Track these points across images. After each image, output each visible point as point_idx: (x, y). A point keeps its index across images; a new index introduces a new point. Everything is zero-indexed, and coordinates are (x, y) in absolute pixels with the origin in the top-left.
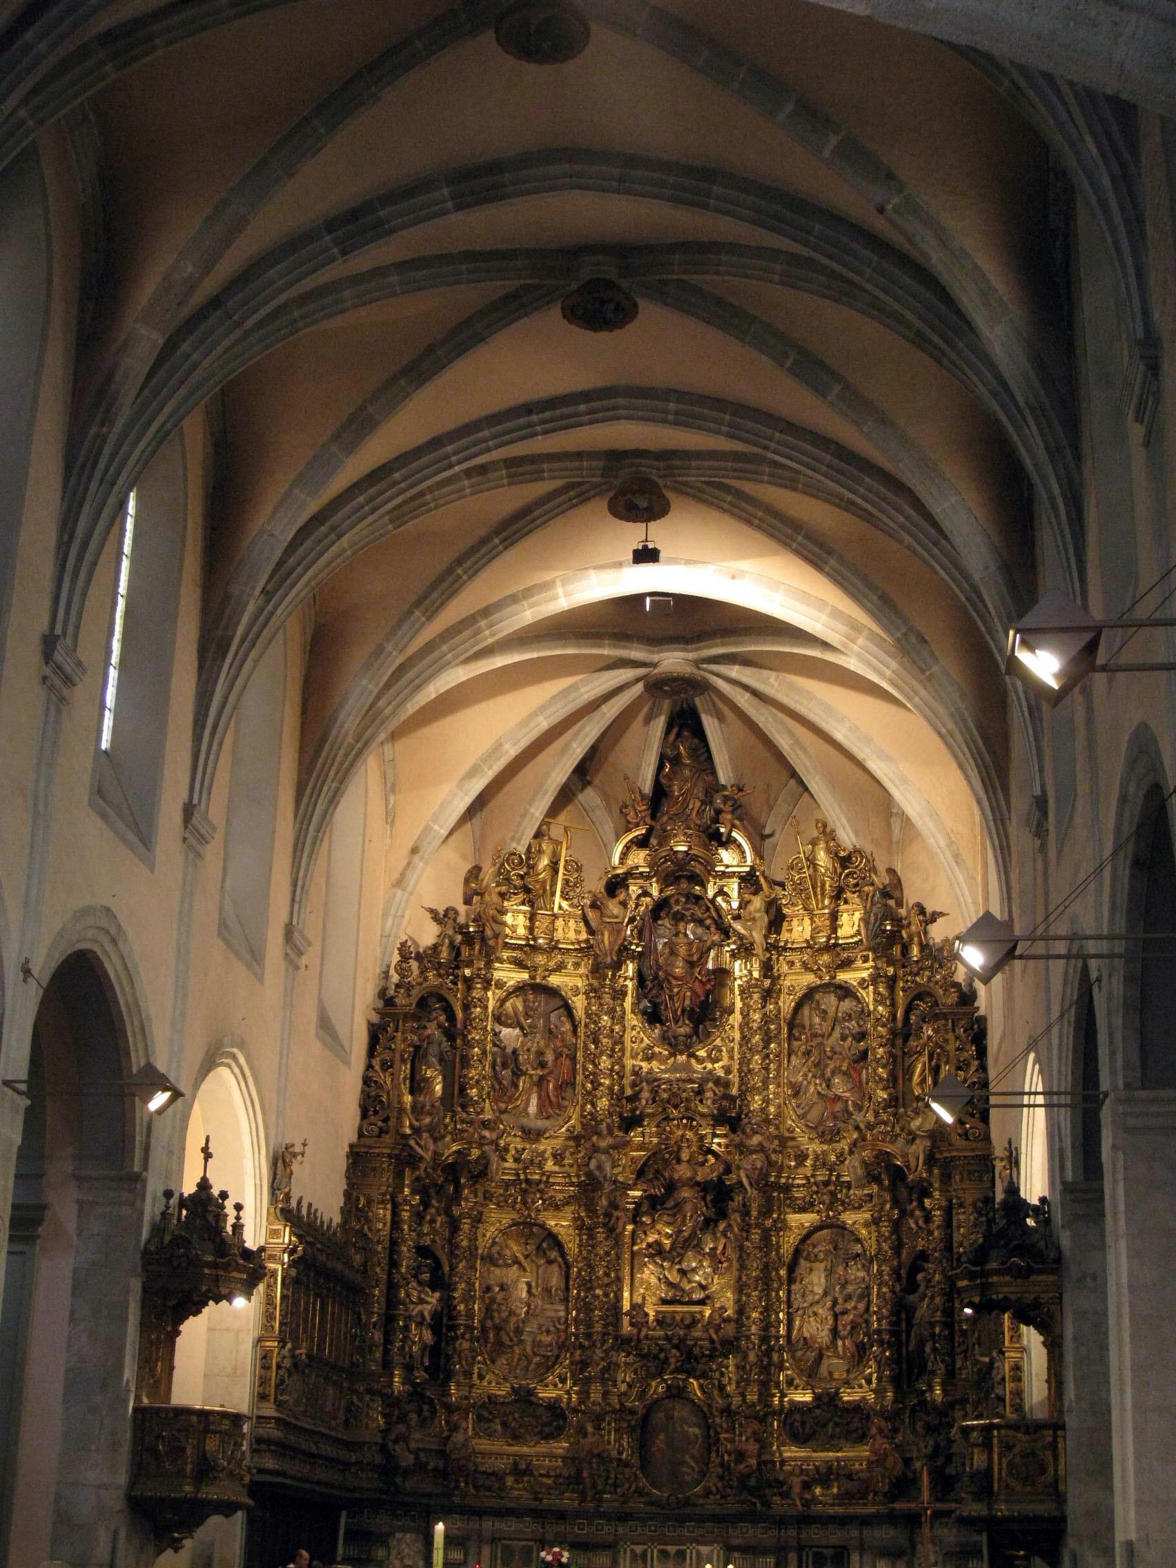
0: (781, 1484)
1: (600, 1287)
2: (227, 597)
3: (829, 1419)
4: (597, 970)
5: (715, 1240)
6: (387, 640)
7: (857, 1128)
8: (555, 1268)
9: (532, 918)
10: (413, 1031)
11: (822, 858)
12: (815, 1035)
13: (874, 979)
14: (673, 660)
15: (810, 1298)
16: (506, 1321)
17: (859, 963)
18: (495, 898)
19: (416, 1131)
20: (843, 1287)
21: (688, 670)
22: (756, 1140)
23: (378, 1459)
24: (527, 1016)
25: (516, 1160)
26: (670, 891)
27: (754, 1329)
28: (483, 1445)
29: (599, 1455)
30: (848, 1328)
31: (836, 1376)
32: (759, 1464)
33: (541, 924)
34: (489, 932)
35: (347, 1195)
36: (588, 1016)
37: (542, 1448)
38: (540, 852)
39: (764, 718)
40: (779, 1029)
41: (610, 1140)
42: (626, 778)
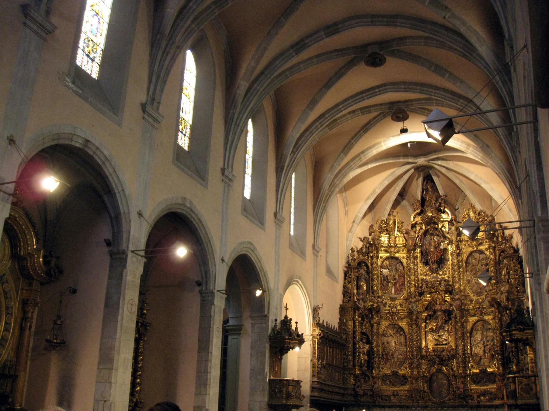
0: (471, 396)
2: (282, 154)
3: (484, 377)
4: (409, 251)
5: (448, 326)
6: (335, 162)
7: (486, 291)
8: (402, 336)
9: (389, 238)
10: (356, 272)
11: (472, 214)
12: (473, 265)
13: (489, 247)
14: (421, 161)
15: (477, 342)
16: (389, 352)
17: (485, 243)
18: (378, 233)
19: (358, 300)
20: (486, 338)
21: (425, 163)
22: (457, 297)
23: (353, 393)
24: (390, 266)
25: (389, 307)
26: (429, 227)
27: (460, 351)
28: (384, 387)
29: (417, 389)
31: (486, 364)
32: (464, 390)
33: (392, 240)
34: (376, 243)
35: (340, 319)
36: (407, 264)
37: (401, 388)
38: (390, 219)
39: (450, 175)
40: (463, 264)
41: (415, 299)
42: (413, 196)
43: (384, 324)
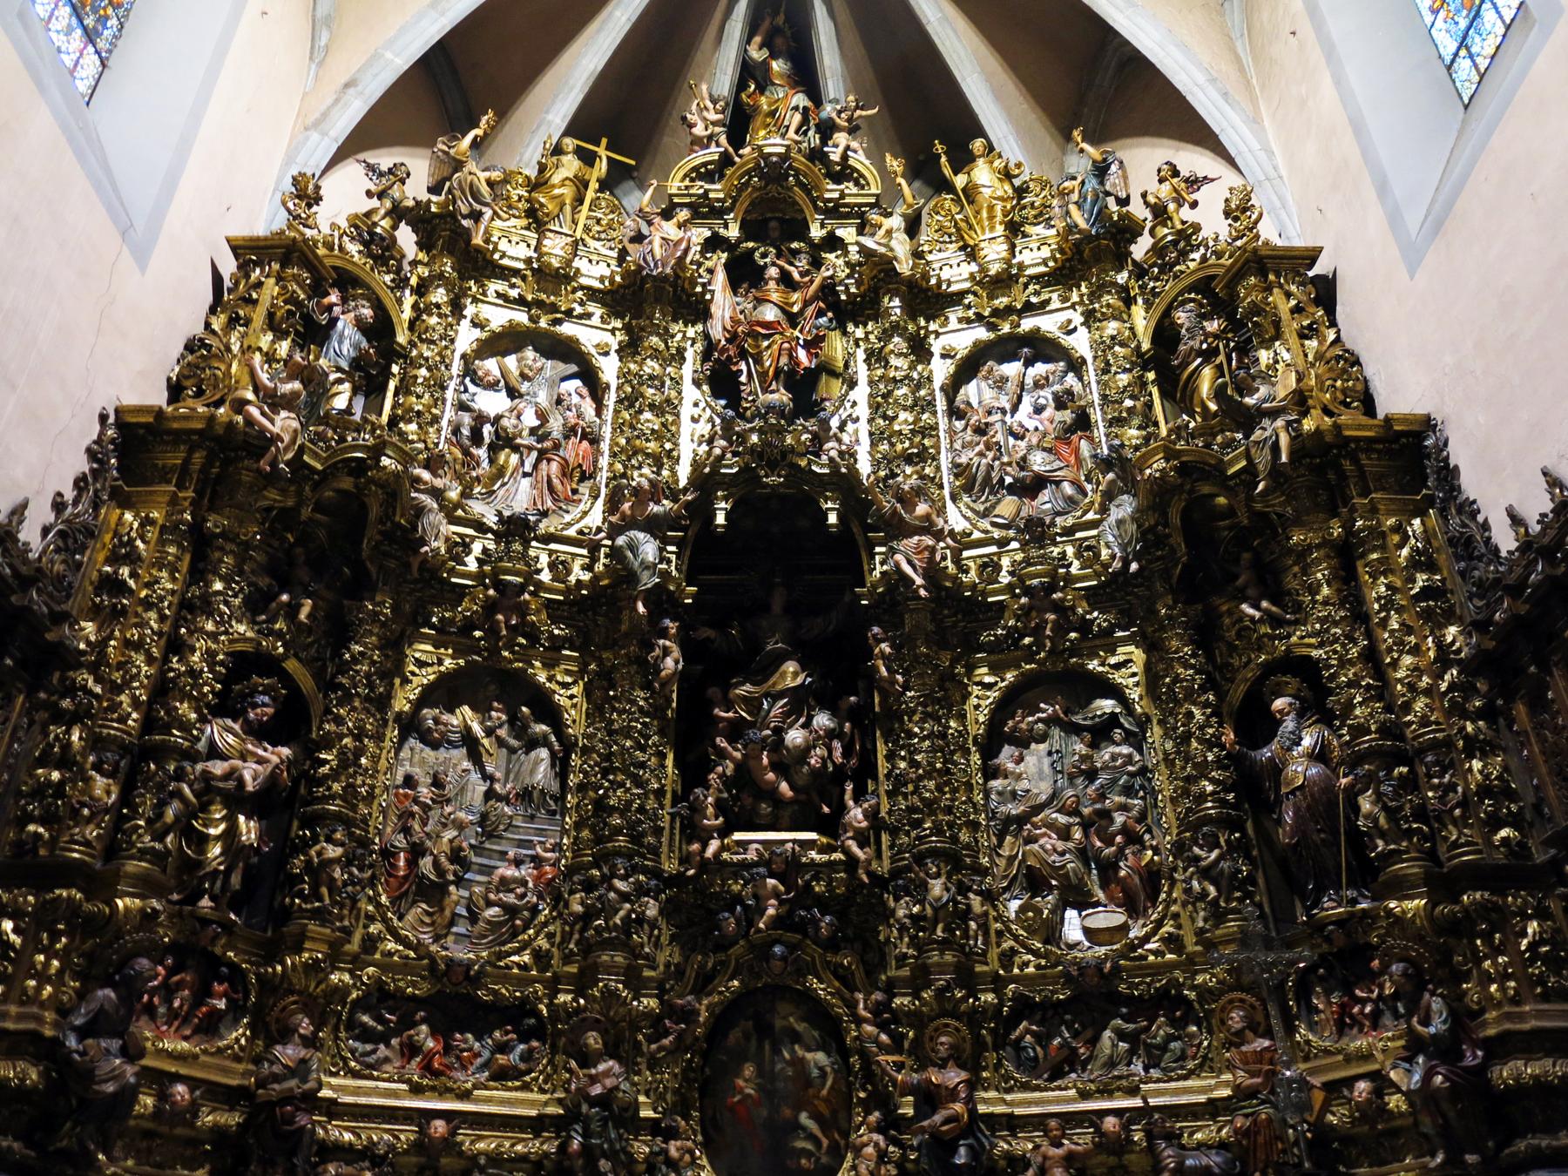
43: (428, 661)
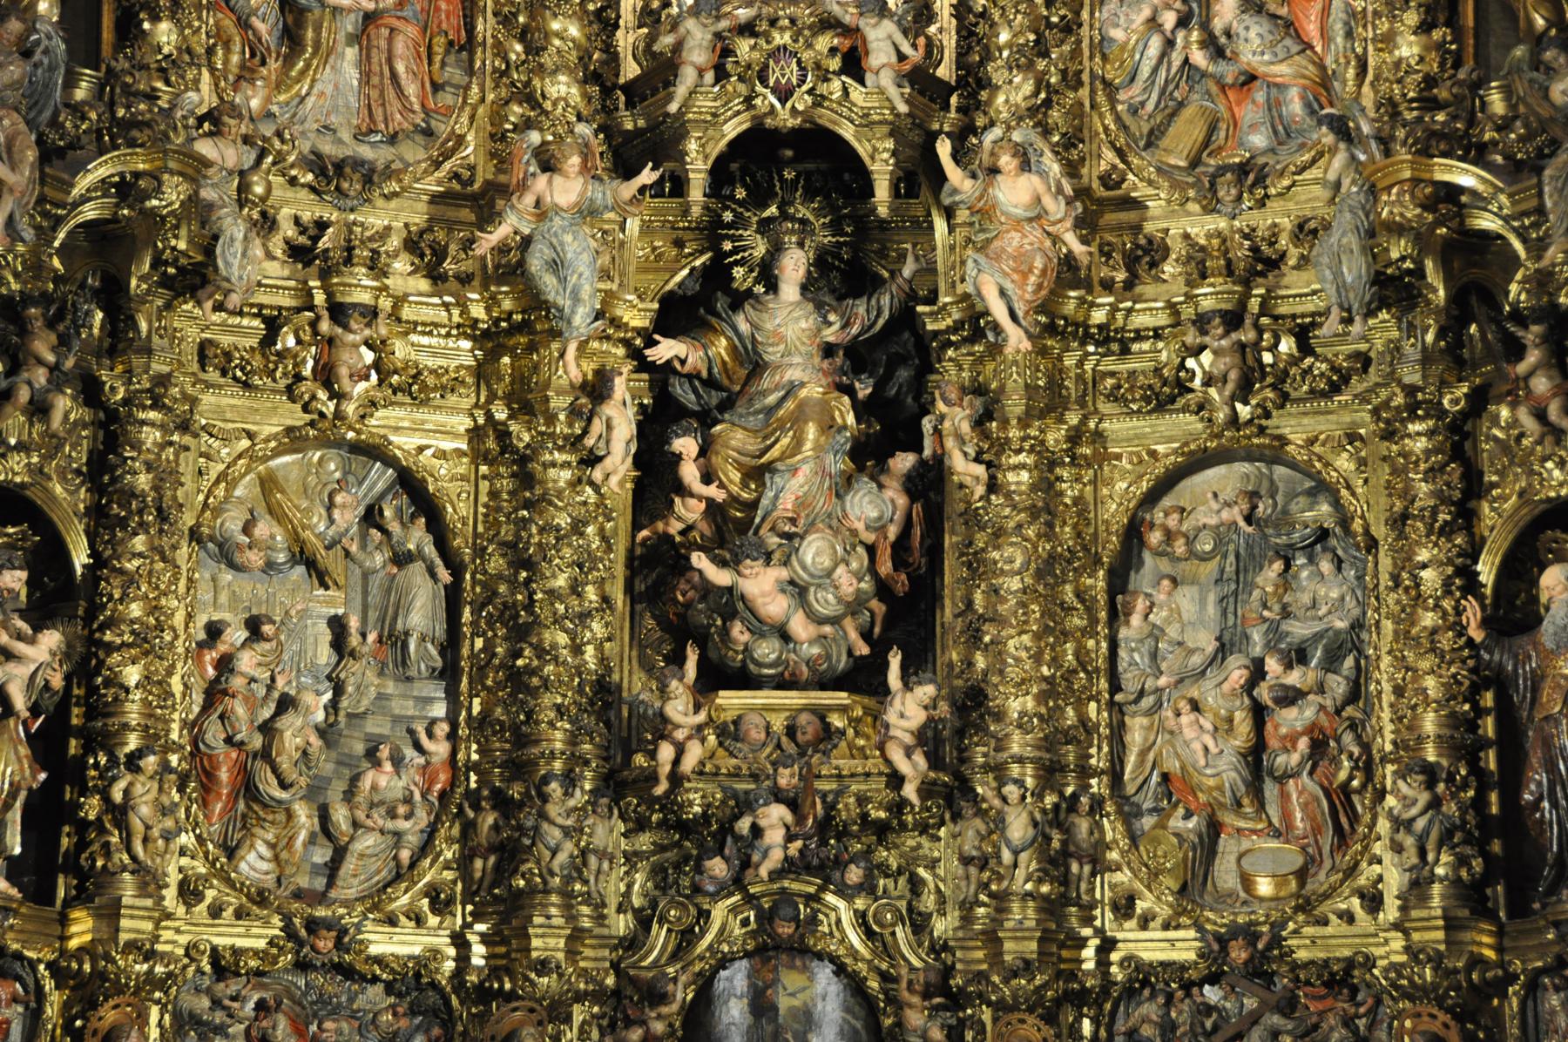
1: (557, 621)
27: (1018, 744)
30: (1303, 744)
